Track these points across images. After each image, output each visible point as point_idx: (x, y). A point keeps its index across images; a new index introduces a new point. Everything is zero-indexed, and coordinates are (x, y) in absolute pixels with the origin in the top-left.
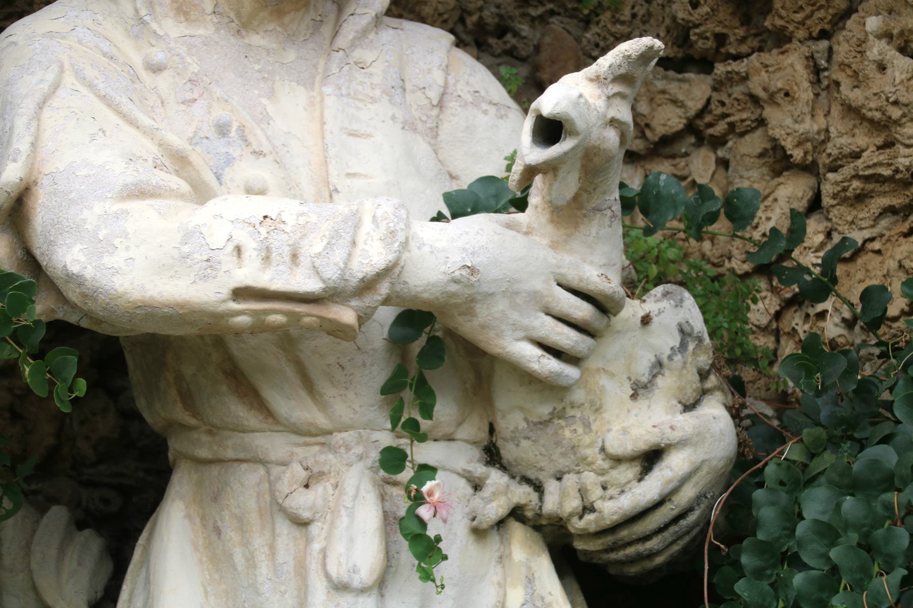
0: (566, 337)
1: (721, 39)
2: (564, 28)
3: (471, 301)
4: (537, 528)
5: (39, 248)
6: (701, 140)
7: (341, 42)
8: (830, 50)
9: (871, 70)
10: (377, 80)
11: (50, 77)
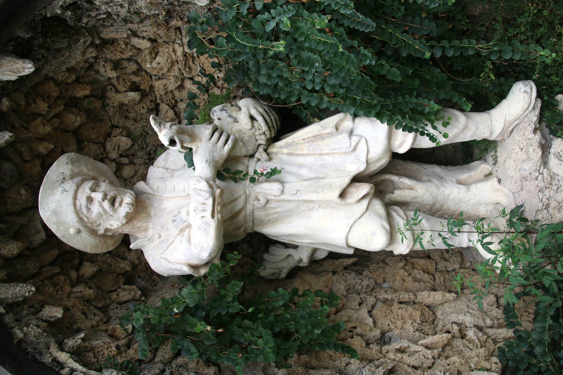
0: (223, 138)
1: (151, 101)
3: (214, 161)
5: (203, 263)
7: (152, 193)
9: (159, 66)
10: (161, 184)
11: (163, 260)
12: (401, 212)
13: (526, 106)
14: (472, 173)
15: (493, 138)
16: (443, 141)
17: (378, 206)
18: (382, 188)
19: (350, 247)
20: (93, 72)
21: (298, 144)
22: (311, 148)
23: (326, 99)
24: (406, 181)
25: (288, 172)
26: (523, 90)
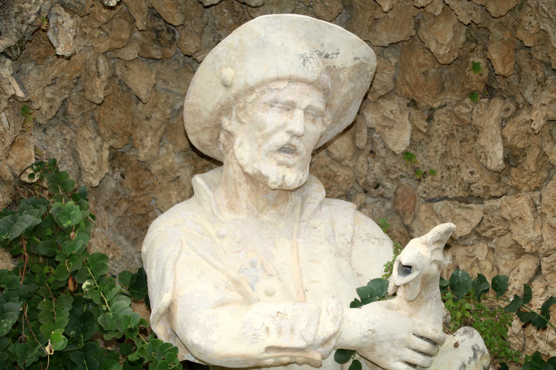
1: (487, 189)
2: (408, 183)
7: (305, 217)
8: (541, 196)
20: (541, 75)
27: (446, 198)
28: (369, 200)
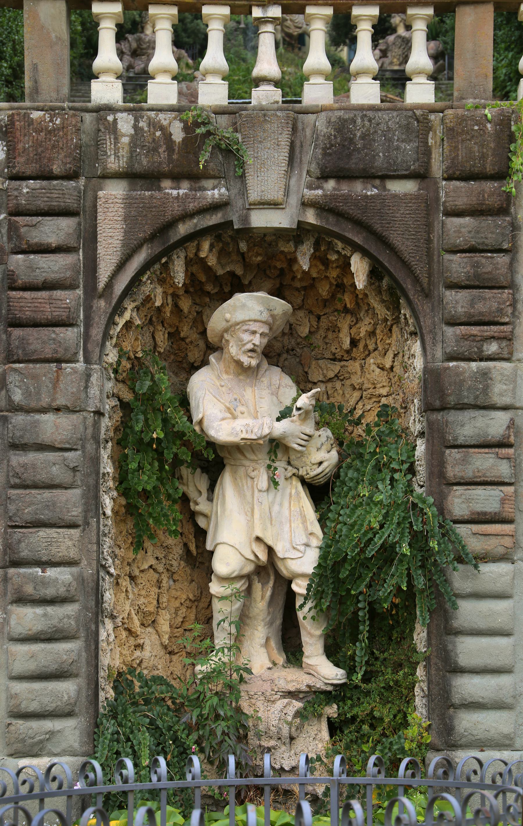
0: (303, 443)
1: (343, 356)
4: (298, 477)
6: (338, 379)
7: (258, 378)
9: (371, 372)
12: (244, 588)
13: (326, 677)
14: (275, 651)
15: (305, 660)
16: (300, 615)
17: (249, 568)
18: (262, 574)
19: (216, 546)
21: (299, 502)
22: (295, 513)
23: (333, 525)
24: (269, 593)
25: (276, 494)
26: (338, 673)
27: (325, 358)
28: (289, 357)
